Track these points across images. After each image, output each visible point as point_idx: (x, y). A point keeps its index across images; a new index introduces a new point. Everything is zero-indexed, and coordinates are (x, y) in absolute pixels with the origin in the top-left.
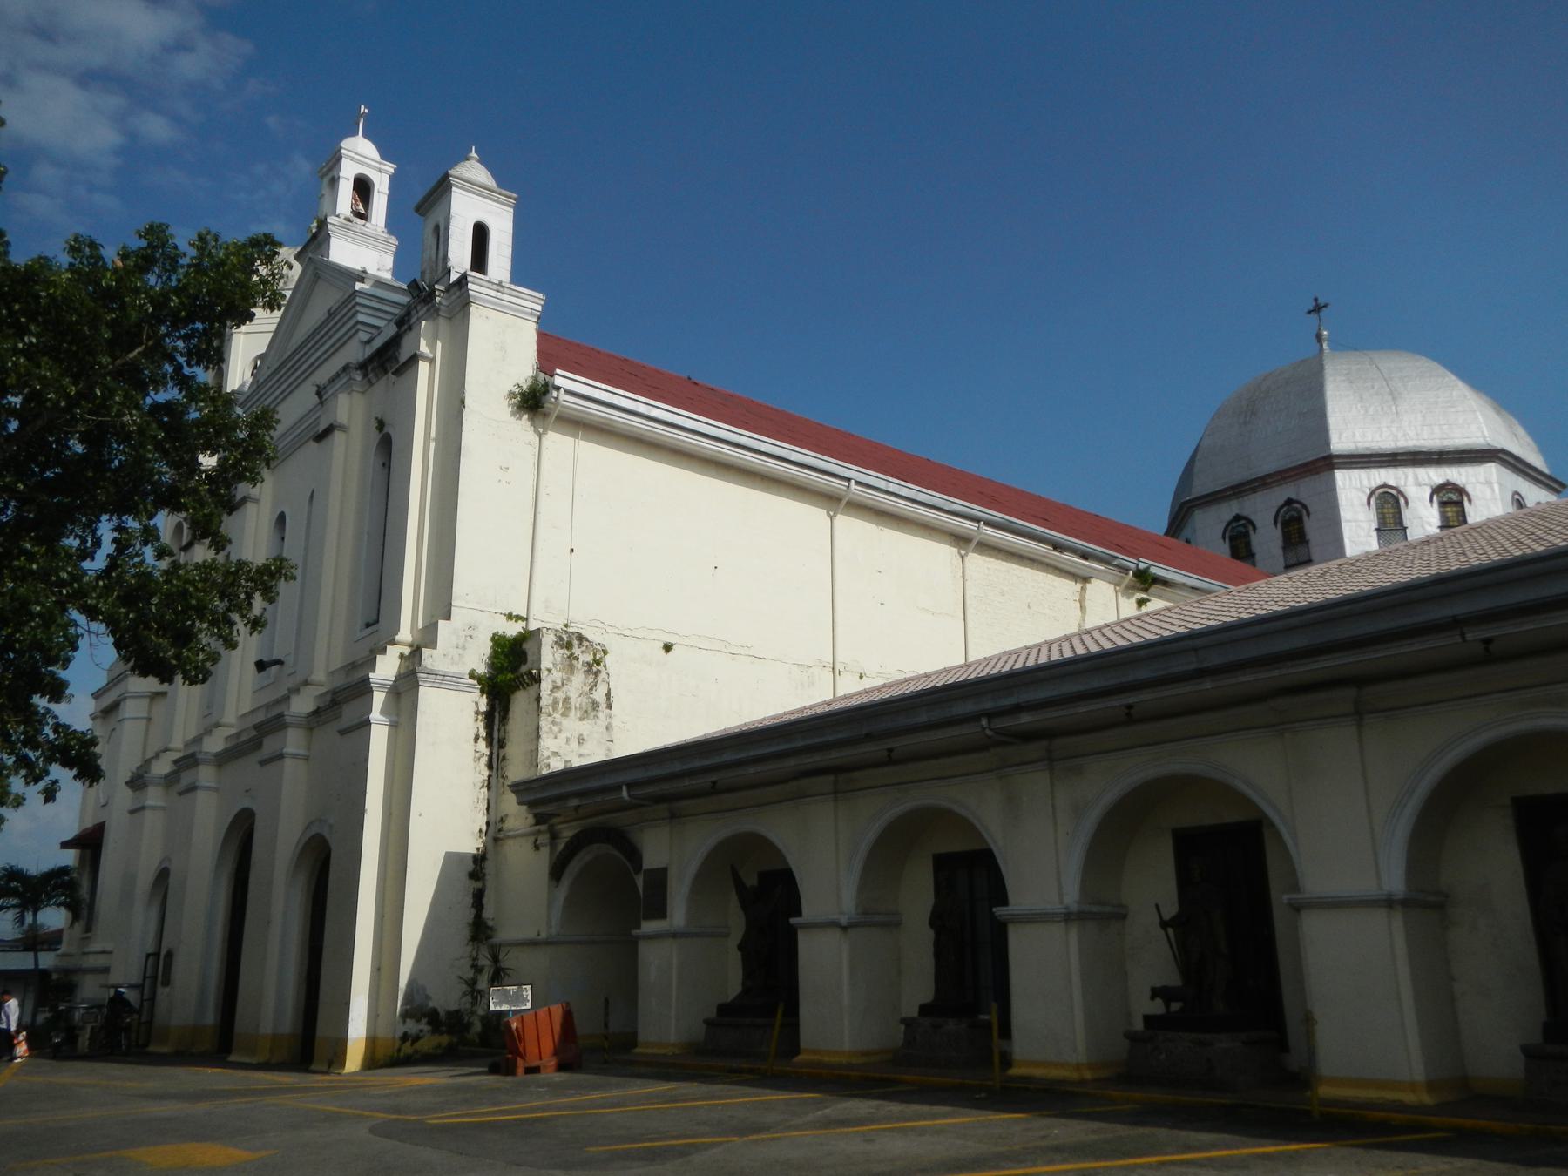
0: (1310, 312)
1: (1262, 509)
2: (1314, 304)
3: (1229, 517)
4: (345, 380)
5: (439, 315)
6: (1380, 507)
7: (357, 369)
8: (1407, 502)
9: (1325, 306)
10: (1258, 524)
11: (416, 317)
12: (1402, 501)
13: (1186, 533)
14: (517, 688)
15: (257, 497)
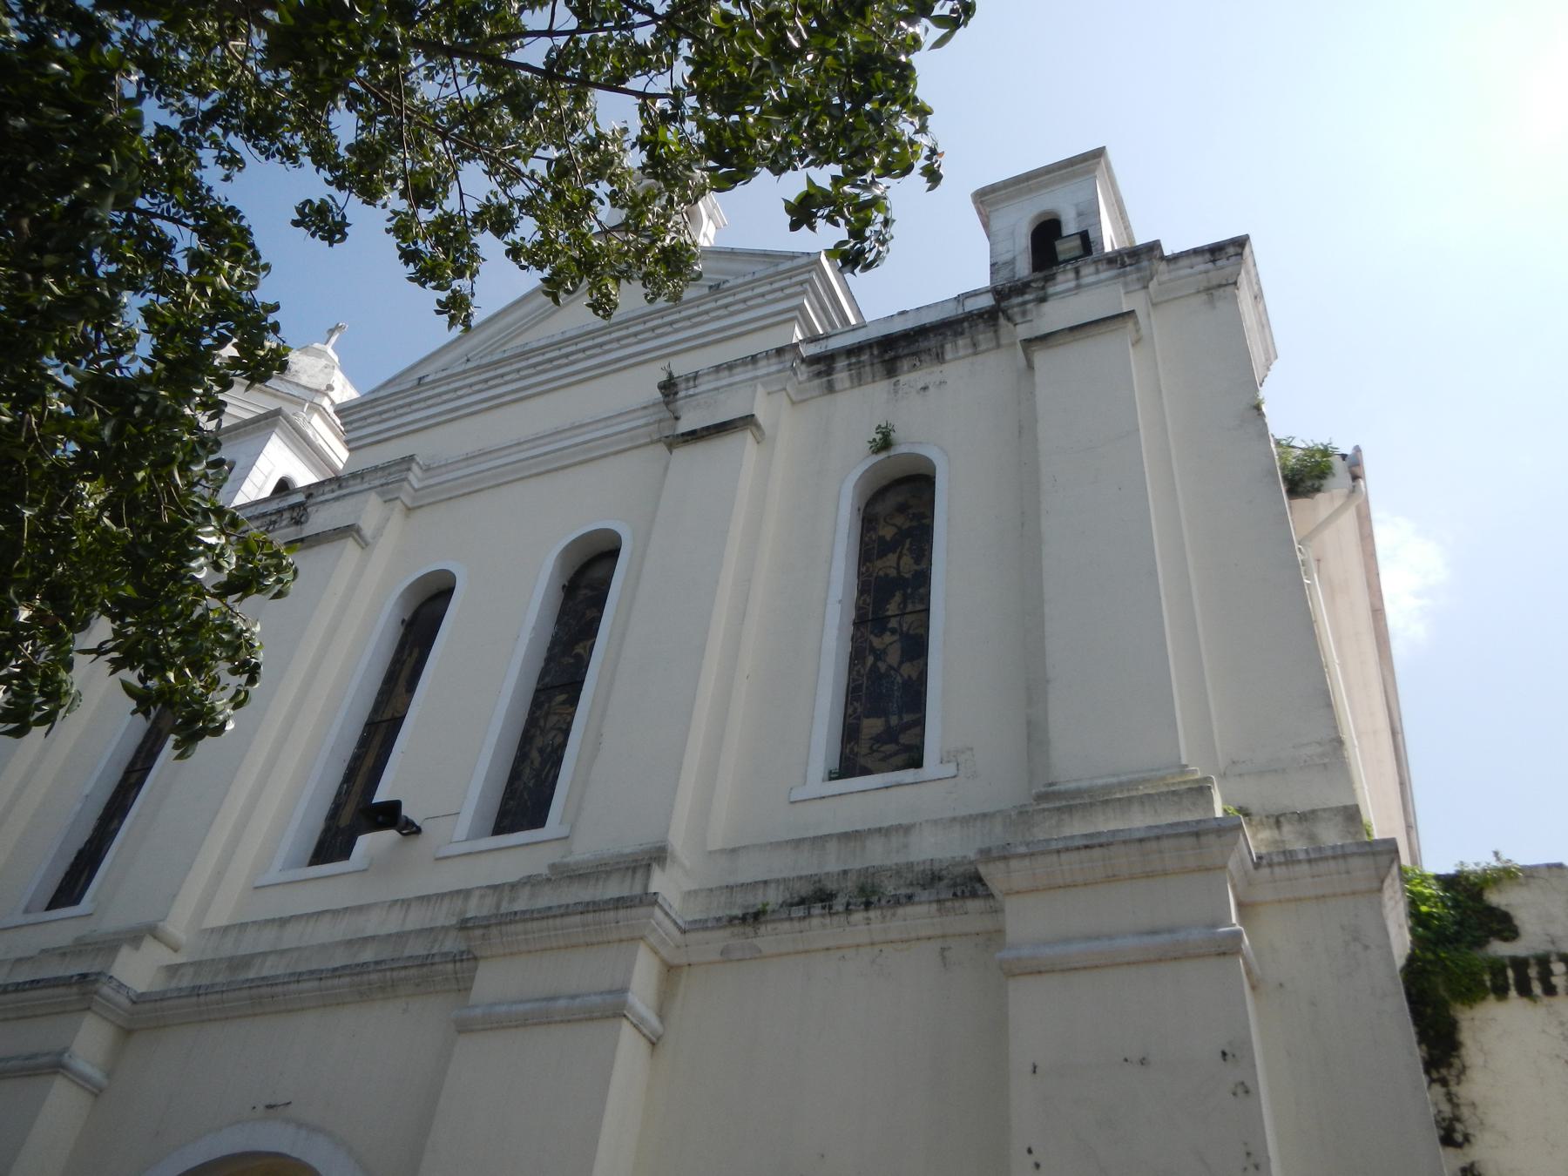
4: (774, 368)
5: (1146, 287)
7: (803, 360)
11: (1072, 284)
14: (1501, 992)
15: (370, 540)
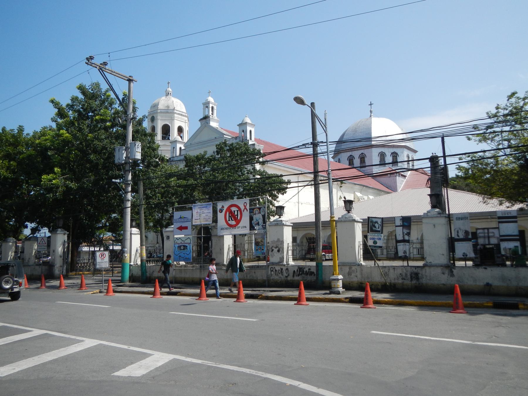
3: (349, 155)
6: (381, 157)
10: (355, 158)
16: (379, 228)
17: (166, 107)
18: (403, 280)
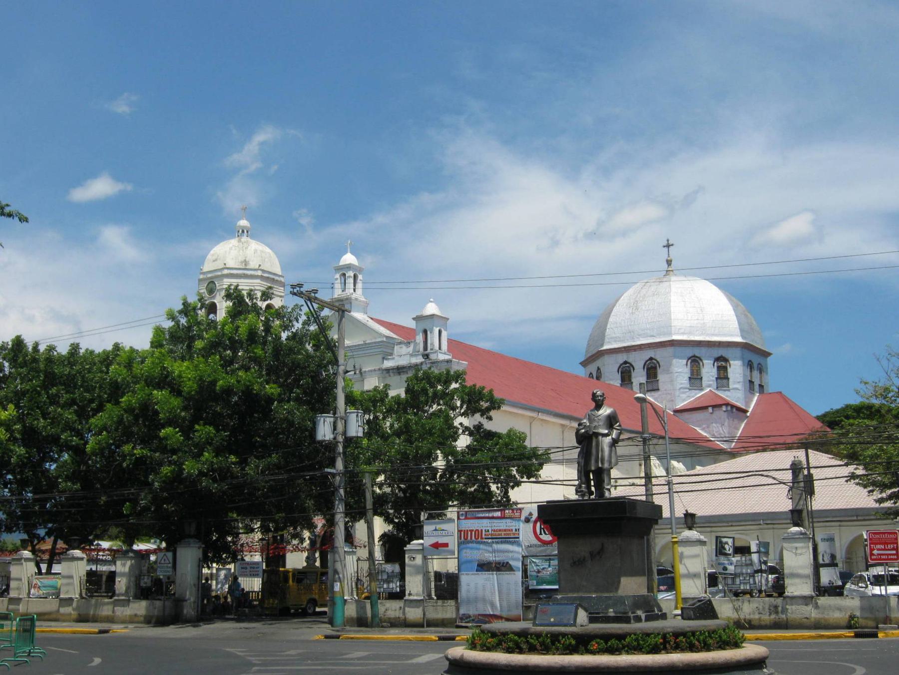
0: (664, 247)
1: (638, 361)
2: (666, 242)
3: (621, 362)
6: (692, 367)
8: (703, 365)
9: (672, 245)
12: (701, 364)
13: (599, 363)
16: (729, 550)
17: (242, 262)
18: (761, 615)
